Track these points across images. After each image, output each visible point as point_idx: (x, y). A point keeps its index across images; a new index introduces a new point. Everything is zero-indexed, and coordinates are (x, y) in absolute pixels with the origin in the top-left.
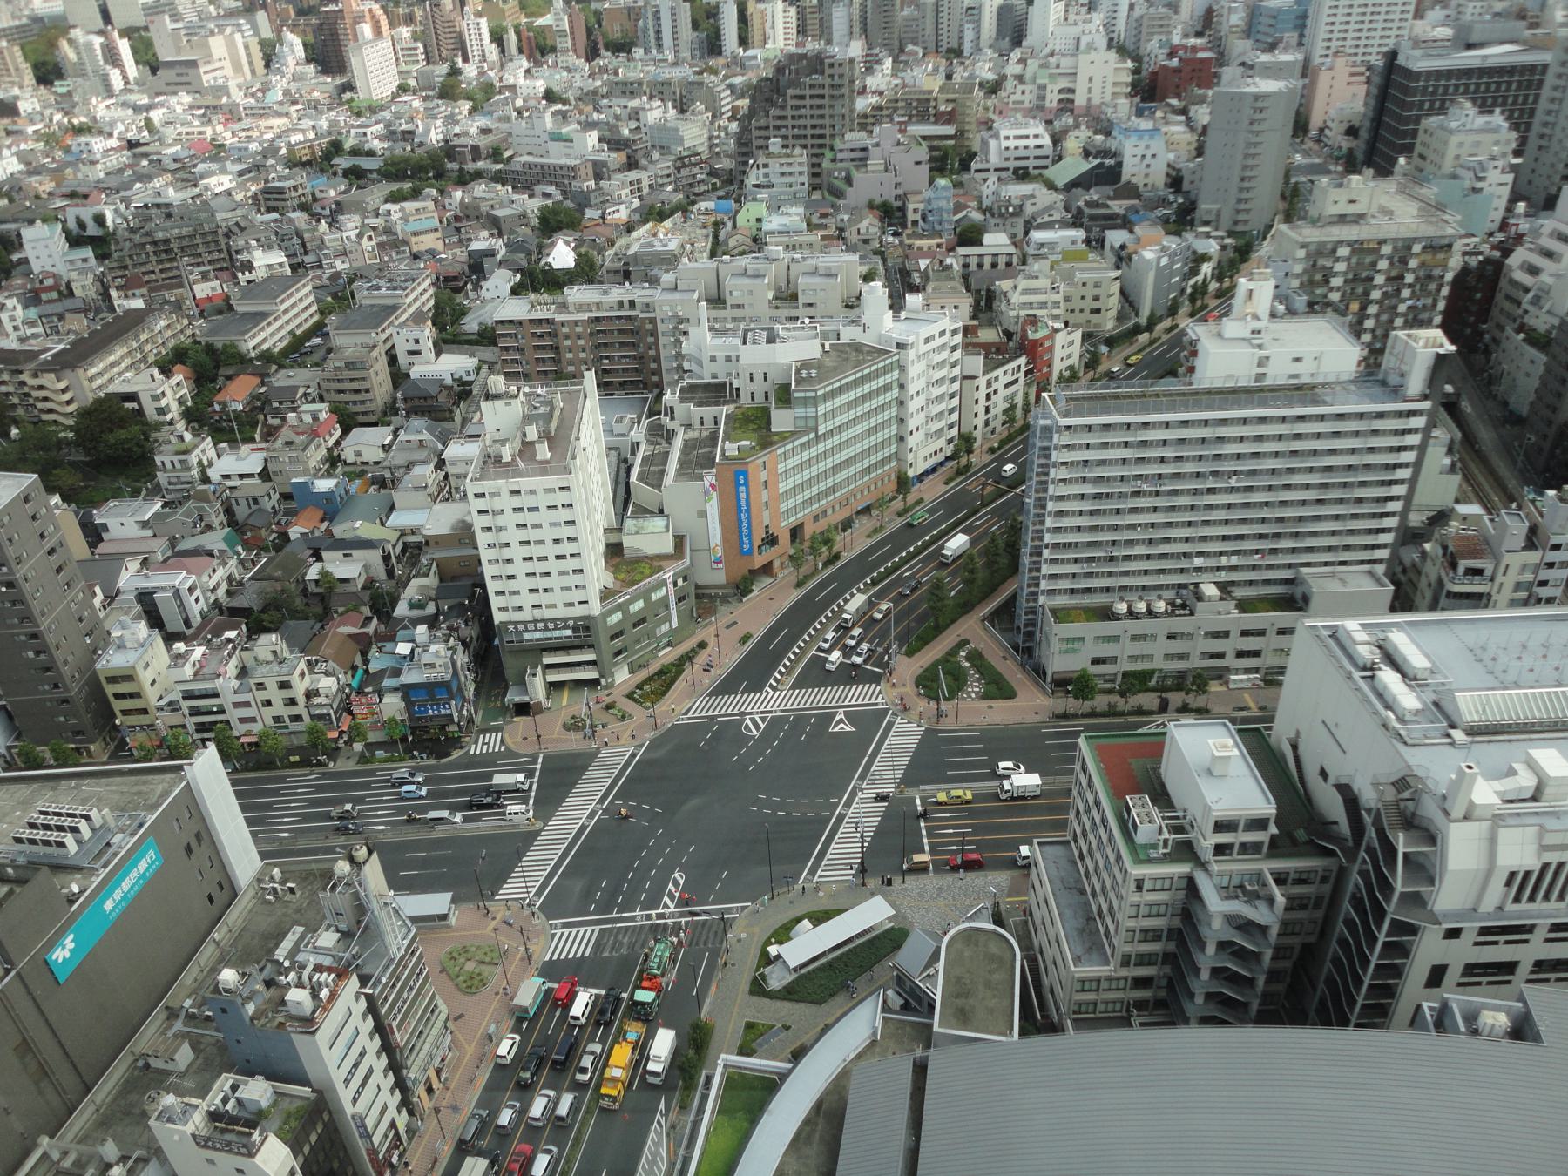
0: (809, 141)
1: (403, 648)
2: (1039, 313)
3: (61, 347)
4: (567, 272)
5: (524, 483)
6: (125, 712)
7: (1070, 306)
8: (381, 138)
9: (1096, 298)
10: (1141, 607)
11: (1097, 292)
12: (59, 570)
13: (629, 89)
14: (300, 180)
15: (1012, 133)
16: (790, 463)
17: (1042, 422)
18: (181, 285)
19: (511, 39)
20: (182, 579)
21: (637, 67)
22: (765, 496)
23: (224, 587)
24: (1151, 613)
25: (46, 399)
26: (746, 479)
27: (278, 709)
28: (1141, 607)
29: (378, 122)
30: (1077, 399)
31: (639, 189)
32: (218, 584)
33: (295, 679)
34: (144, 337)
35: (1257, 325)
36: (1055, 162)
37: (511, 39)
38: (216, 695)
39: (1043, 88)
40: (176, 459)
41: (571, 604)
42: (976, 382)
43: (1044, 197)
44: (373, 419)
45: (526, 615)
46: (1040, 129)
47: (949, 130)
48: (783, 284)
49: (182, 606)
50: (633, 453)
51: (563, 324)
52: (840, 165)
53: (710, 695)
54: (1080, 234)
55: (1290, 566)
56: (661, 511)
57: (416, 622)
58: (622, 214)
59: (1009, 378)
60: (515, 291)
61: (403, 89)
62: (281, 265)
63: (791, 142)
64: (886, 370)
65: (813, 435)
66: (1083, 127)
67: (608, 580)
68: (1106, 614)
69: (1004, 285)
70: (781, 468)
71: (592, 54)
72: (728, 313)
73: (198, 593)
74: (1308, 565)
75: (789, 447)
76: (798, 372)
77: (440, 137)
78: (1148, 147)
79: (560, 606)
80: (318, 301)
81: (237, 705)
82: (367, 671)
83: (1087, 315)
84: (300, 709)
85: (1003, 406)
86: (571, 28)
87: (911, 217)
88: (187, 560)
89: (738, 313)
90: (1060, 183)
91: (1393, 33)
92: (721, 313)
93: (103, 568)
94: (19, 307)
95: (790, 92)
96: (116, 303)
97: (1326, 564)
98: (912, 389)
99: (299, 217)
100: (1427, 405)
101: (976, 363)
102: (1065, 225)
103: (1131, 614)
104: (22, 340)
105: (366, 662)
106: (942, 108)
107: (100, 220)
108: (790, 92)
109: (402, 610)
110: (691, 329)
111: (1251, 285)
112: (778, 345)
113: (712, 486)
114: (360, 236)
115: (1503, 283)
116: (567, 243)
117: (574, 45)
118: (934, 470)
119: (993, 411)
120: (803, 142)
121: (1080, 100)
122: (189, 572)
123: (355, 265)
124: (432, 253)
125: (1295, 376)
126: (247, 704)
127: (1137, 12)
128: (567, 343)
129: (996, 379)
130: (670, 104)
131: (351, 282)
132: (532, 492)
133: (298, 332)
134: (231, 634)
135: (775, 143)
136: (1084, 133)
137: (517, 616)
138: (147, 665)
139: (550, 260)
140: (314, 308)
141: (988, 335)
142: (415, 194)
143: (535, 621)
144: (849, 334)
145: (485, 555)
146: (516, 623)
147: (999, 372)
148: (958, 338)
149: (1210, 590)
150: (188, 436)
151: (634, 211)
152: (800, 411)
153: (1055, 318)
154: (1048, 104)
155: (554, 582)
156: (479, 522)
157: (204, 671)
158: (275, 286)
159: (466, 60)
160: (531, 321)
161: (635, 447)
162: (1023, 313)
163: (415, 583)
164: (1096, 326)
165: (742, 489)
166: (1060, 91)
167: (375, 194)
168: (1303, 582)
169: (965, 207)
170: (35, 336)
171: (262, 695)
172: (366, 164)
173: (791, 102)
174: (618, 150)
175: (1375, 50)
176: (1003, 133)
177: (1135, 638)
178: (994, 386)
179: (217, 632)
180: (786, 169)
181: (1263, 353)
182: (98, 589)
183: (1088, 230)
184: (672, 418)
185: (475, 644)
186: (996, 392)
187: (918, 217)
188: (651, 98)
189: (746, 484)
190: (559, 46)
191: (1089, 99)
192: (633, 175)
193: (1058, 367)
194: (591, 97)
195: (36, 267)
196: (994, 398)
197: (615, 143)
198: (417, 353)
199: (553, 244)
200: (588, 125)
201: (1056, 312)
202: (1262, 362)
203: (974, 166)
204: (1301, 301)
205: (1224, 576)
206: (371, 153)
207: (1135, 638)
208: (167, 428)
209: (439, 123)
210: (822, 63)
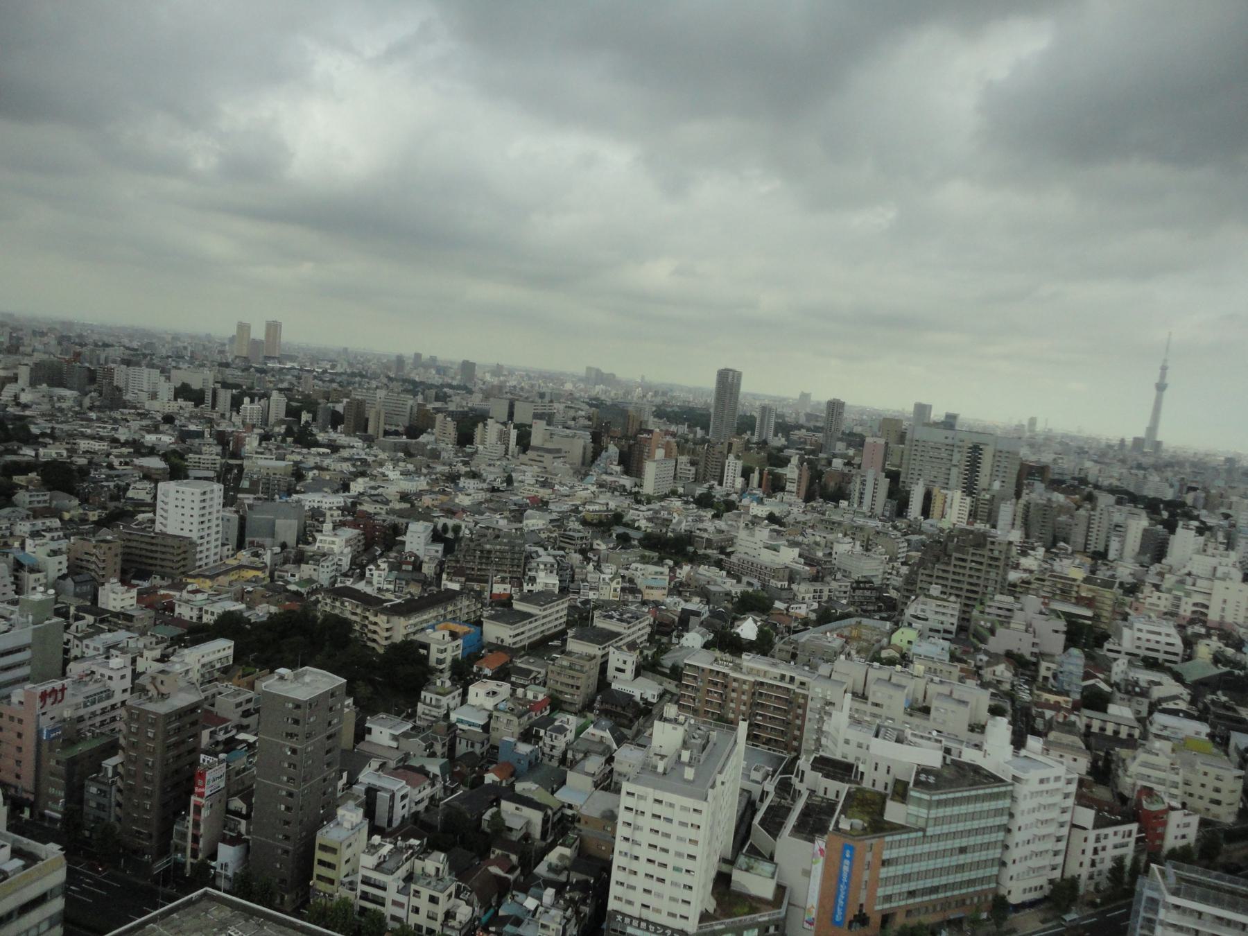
0: (964, 594)
1: (530, 903)
2: (1156, 787)
3: (399, 601)
4: (751, 642)
5: (666, 797)
6: (320, 878)
7: (1188, 789)
8: (649, 520)
11: (1218, 784)
12: (328, 752)
14: (586, 534)
15: (1146, 627)
17: (1148, 893)
18: (486, 582)
19: (755, 477)
20: (399, 786)
21: (842, 512)
22: (866, 875)
23: (426, 803)
25: (375, 632)
27: (421, 919)
29: (649, 510)
30: (1188, 881)
31: (820, 597)
32: (422, 800)
33: (442, 897)
34: (450, 608)
36: (1184, 660)
37: (755, 477)
38: (384, 889)
39: (1178, 598)
40: (434, 697)
41: (674, 915)
43: (1168, 687)
44: (573, 709)
45: (635, 911)
46: (1173, 631)
47: (1089, 613)
48: (920, 698)
49: (391, 808)
50: (762, 800)
51: (735, 680)
52: (986, 616)
54: (1205, 729)
56: (771, 859)
57: (548, 883)
58: (802, 611)
59: (1118, 840)
60: (707, 646)
61: (674, 493)
62: (554, 584)
63: (948, 590)
65: (920, 834)
66: (1215, 638)
67: (711, 906)
71: (809, 498)
72: (868, 708)
73: (406, 801)
75: (897, 837)
76: (918, 773)
77: (688, 528)
79: (665, 913)
80: (568, 615)
81: (395, 903)
82: (497, 912)
83: (1205, 803)
84: (437, 926)
85: (1109, 864)
87: (1043, 672)
88: (410, 773)
89: (876, 710)
90: (1189, 680)
92: (862, 707)
93: (353, 762)
94: (387, 570)
96: (443, 582)
98: (1020, 820)
99: (576, 558)
101: (1087, 816)
102: (1188, 715)
104: (379, 589)
105: (499, 904)
106: (1083, 594)
107: (457, 529)
108: (955, 555)
109: (541, 869)
110: (834, 713)
113: (821, 850)
114: (612, 580)
116: (755, 622)
117: (798, 489)
118: (1031, 904)
119: (1099, 867)
121: (1213, 616)
122: (407, 783)
123: (602, 598)
124: (657, 604)
126: (401, 905)
128: (734, 695)
129: (1106, 837)
130: (858, 543)
131: (595, 608)
132: (671, 805)
133: (546, 633)
134: (414, 842)
135: (935, 590)
136: (1215, 643)
137: (627, 909)
138: (350, 845)
139: (738, 630)
140: (565, 619)
141: (1102, 793)
142: (660, 562)
143: (640, 920)
144: (970, 756)
145: (619, 845)
146: (624, 915)
147: (1109, 831)
148: (1073, 788)
150: (448, 683)
151: (814, 611)
152: (912, 809)
153: (1173, 796)
154: (1181, 612)
155: (666, 889)
156: (623, 816)
157: (384, 865)
158: (543, 598)
159: (721, 484)
160: (711, 671)
161: (764, 794)
162: (1140, 783)
163: (559, 850)
164: (1215, 816)
165: (847, 862)
166: (1195, 605)
167: (632, 555)
169: (1097, 677)
170: (388, 590)
171: (415, 902)
172: (632, 533)
173: (954, 562)
176: (1137, 625)
178: (1103, 842)
179: (405, 838)
180: (939, 609)
182: (345, 775)
183: (1213, 726)
184: (802, 781)
185: (586, 921)
186: (1104, 849)
187: (1049, 674)
188: (845, 535)
190: (787, 488)
191: (1222, 617)
192: (818, 586)
193: (1171, 840)
194: (801, 527)
195: (408, 548)
196: (1101, 854)
197: (810, 561)
198: (623, 671)
199: (745, 619)
201: (1174, 791)
203: (1107, 646)
206: (638, 528)
208: (438, 674)
209: (690, 519)
210: (985, 540)
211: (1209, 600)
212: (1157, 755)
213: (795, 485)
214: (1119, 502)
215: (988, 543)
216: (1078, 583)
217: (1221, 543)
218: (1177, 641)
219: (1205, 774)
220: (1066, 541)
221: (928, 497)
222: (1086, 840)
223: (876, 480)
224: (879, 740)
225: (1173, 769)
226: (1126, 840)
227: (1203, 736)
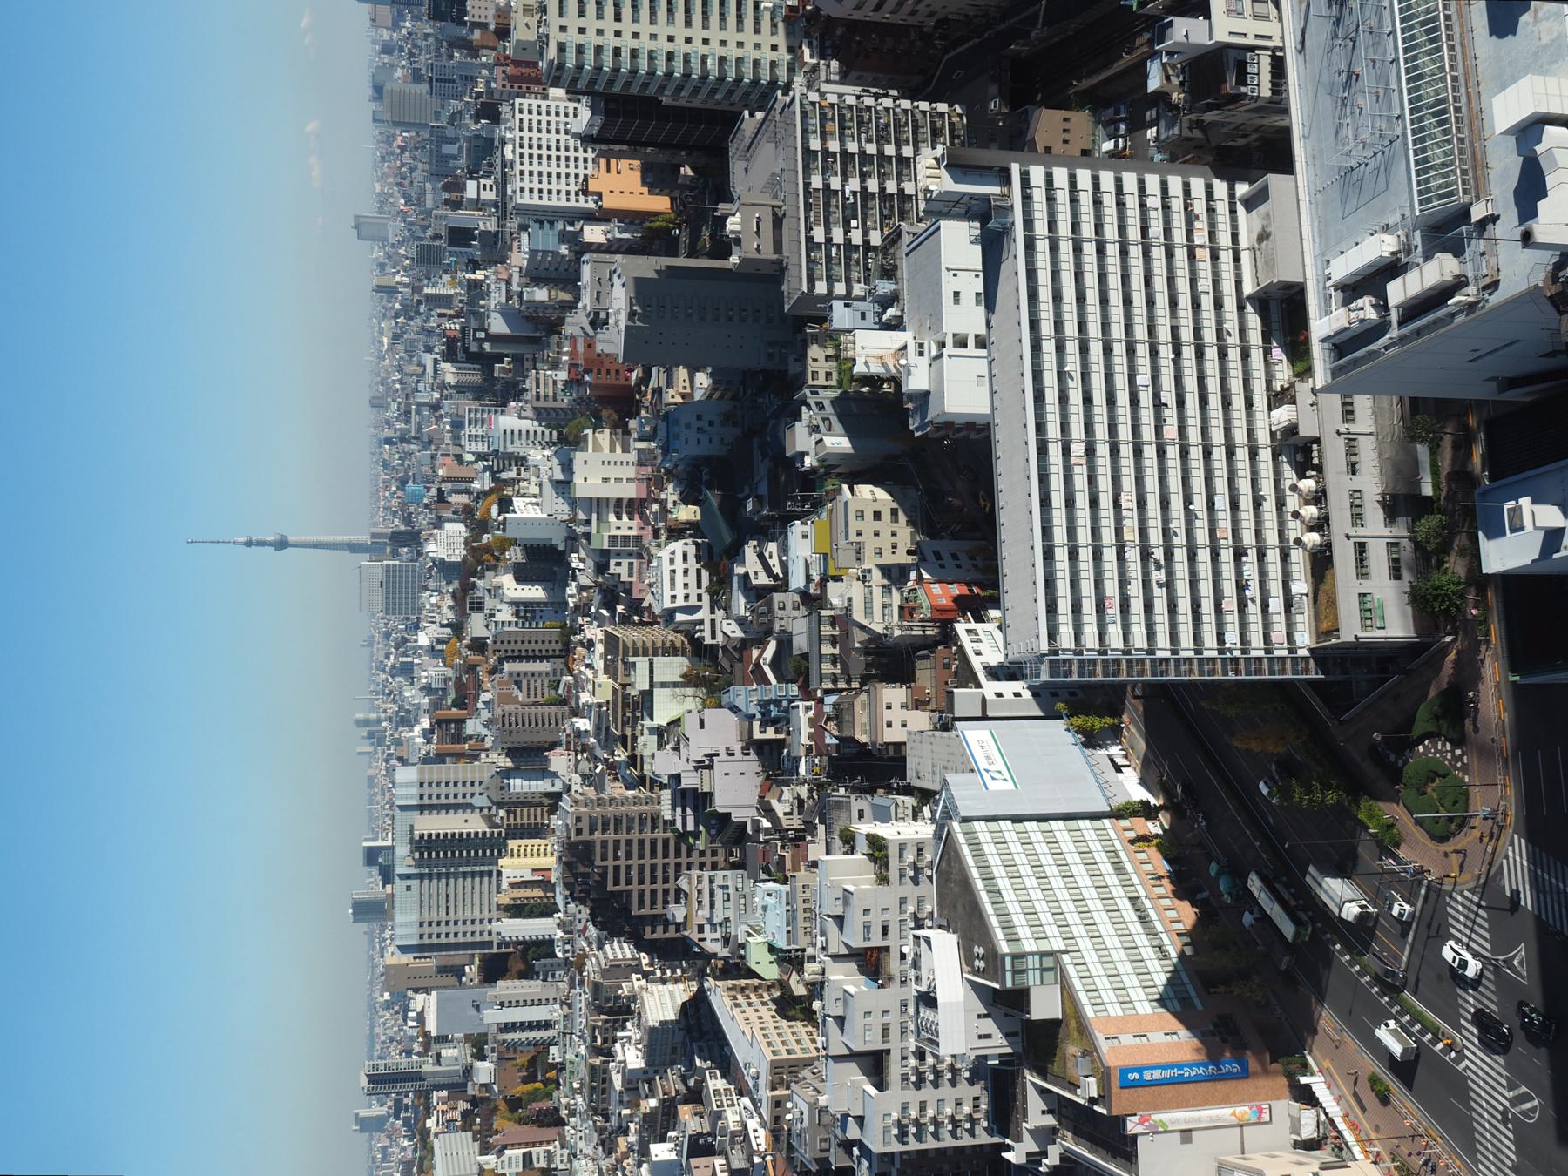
0: (672, 860)
9: (877, 516)
10: (1311, 511)
11: (869, 516)
13: (599, 1078)
15: (667, 594)
16: (1108, 996)
21: (573, 1053)
24: (1319, 498)
26: (1133, 1070)
28: (1311, 511)
35: (912, 349)
42: (990, 696)
46: (665, 554)
53: (1476, 1162)
55: (1241, 308)
64: (975, 844)
65: (1066, 958)
68: (1321, 562)
69: (858, 638)
70: (1115, 1010)
72: (894, 1045)
74: (1239, 284)
76: (977, 972)
78: (688, 426)
86: (520, 1145)
89: (895, 1032)
91: (562, 137)
95: (610, 887)
97: (1237, 259)
100: (1015, 169)
103: (1321, 524)
108: (610, 887)
111: (860, 361)
112: (941, 998)
113: (1141, 1122)
115: (857, 16)
117: (541, 1143)
120: (671, 871)
121: (630, 491)
125: (978, 294)
127: (529, 413)
130: (619, 1034)
149: (1283, 415)
152: (1032, 979)
154: (633, 533)
165: (1147, 1076)
166: (619, 517)
168: (1265, 290)
169: (758, 665)
173: (622, 887)
174: (676, 1115)
175: (581, 155)
176: (668, 604)
177: (1357, 517)
181: (949, 341)
188: (610, 1054)
189: (1140, 1070)
200: (644, 1152)
202: (961, 343)
203: (708, 641)
204: (885, 287)
205: (1260, 402)
207: (1357, 517)
211: (608, 499)
212: (850, 599)
213: (534, 1150)
214: (478, 607)
215: (580, 838)
216: (618, 687)
217: (519, 474)
218: (678, 546)
219: (859, 534)
220: (557, 688)
221: (517, 910)
222: (999, 695)
223: (502, 1004)
224: (941, 1040)
225: (864, 577)
226: (982, 636)
227: (807, 528)
